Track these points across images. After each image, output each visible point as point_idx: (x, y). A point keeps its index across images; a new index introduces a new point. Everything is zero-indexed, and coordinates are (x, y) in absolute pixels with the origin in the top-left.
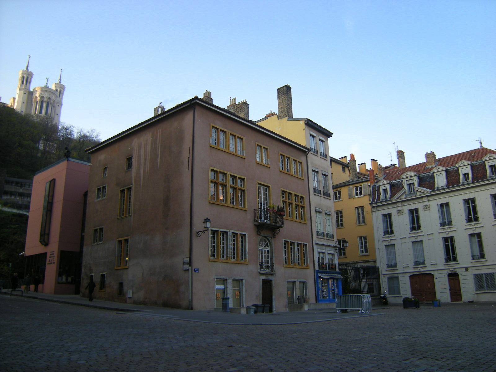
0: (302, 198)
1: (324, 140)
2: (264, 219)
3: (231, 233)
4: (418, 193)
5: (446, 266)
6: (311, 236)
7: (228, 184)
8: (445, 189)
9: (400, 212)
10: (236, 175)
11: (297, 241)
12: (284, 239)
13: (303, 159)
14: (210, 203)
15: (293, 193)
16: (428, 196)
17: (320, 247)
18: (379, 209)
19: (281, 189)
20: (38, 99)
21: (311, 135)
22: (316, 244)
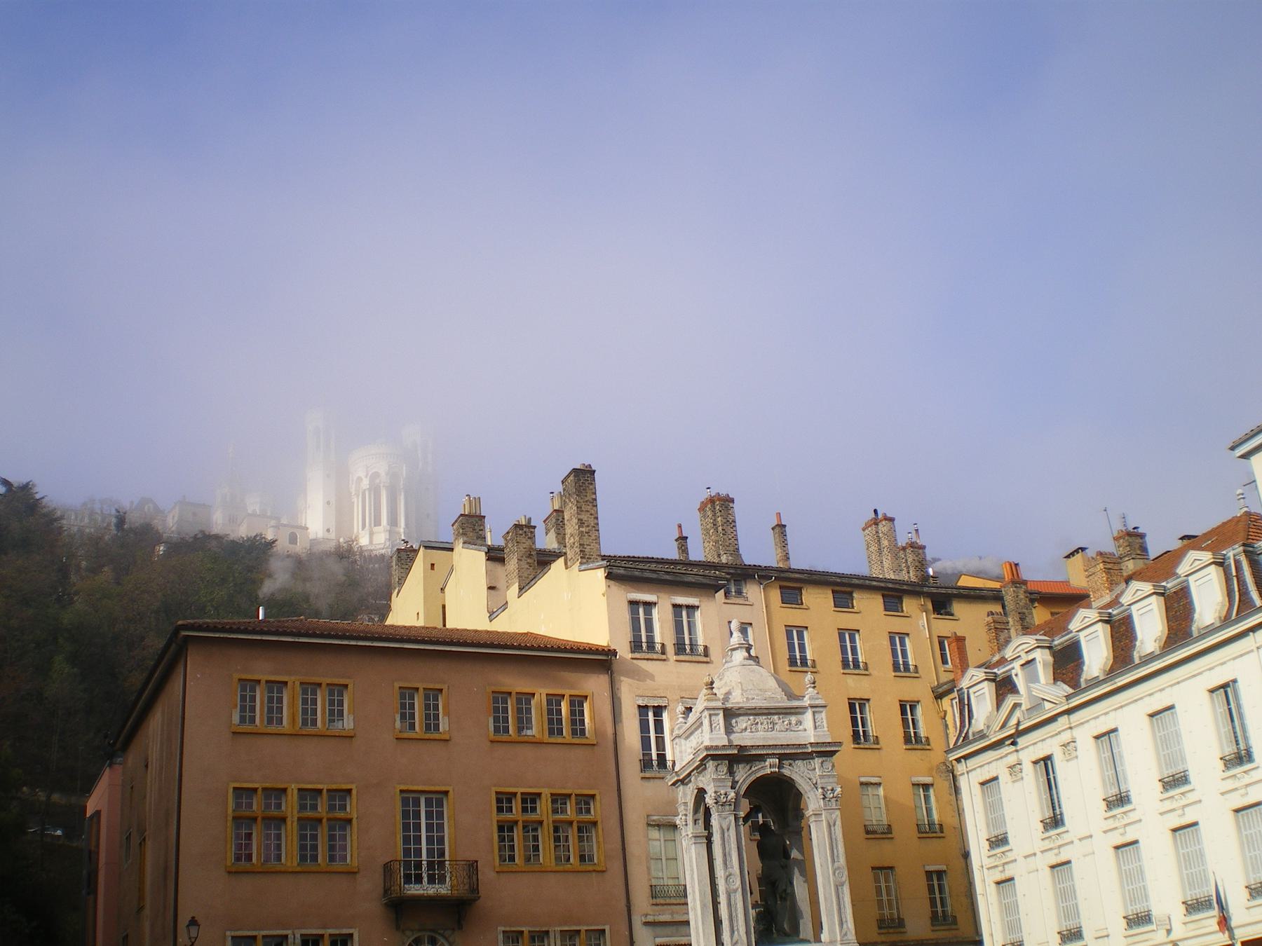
0: (585, 800)
1: (697, 603)
2: (431, 880)
3: (298, 936)
4: (1047, 705)
5: (1192, 926)
6: (624, 902)
7: (289, 815)
8: (1104, 681)
9: (1014, 768)
10: (320, 787)
11: (560, 925)
12: (501, 928)
13: (595, 685)
14: (229, 872)
15: (546, 792)
16: (1069, 712)
17: (659, 930)
18: (972, 763)
19: (494, 789)
20: (365, 483)
21: (634, 604)
22: (646, 924)
